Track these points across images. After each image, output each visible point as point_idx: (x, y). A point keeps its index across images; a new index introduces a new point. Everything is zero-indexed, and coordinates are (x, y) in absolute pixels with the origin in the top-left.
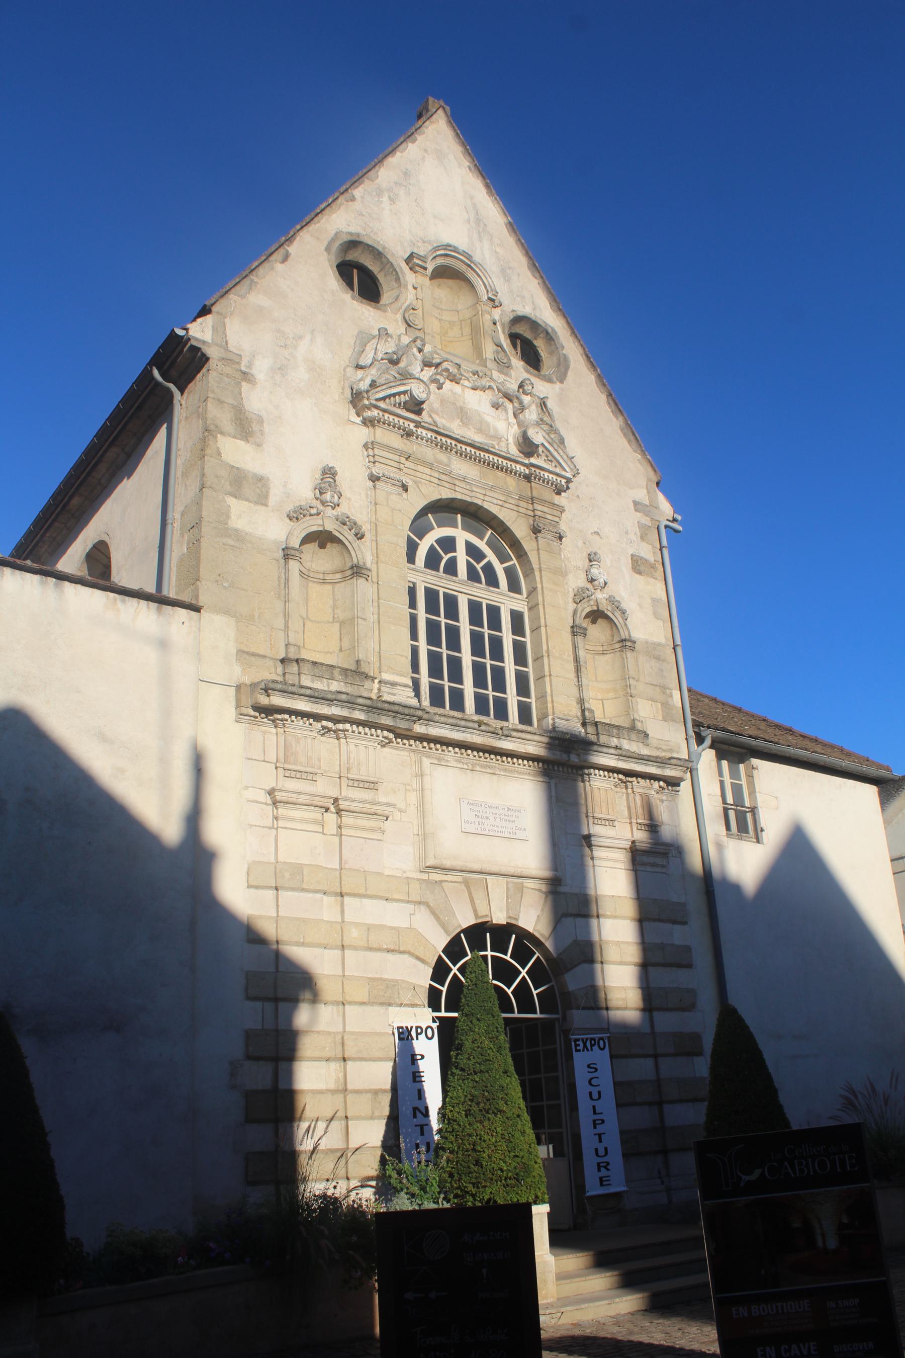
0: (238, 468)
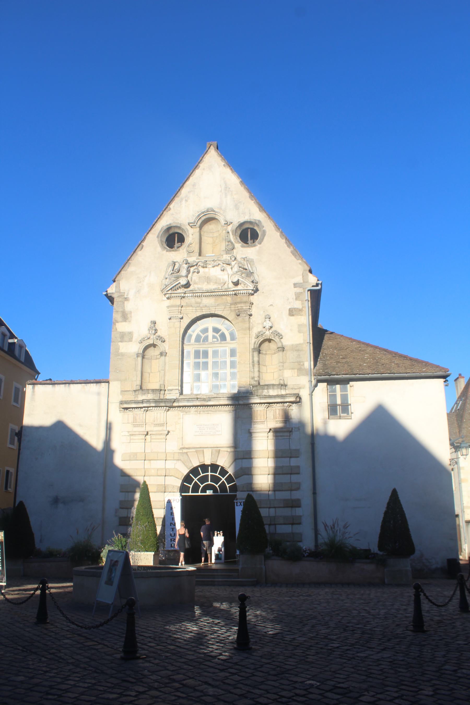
0: (123, 332)
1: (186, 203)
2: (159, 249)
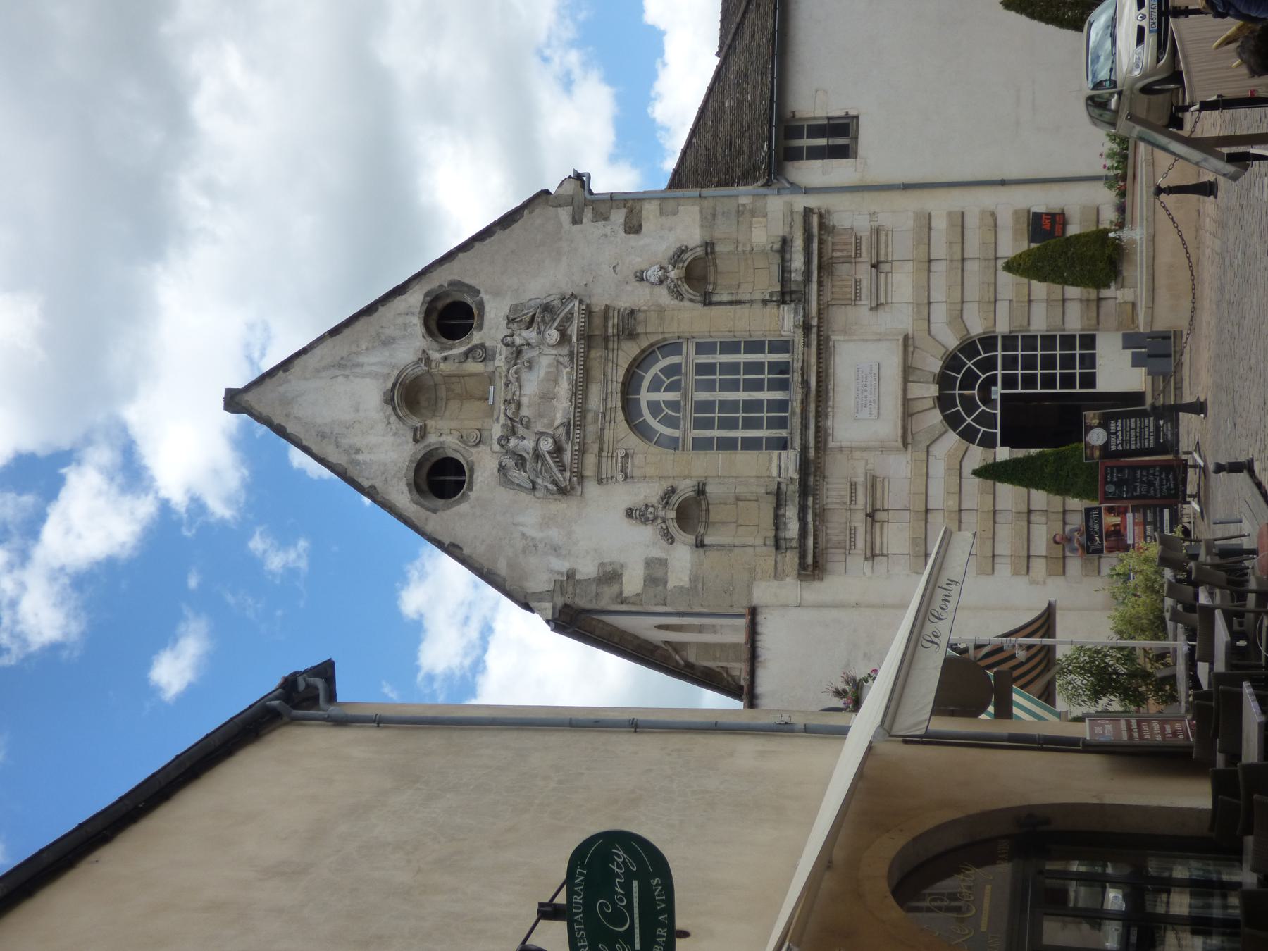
0: (645, 581)
1: (362, 452)
2: (464, 507)
